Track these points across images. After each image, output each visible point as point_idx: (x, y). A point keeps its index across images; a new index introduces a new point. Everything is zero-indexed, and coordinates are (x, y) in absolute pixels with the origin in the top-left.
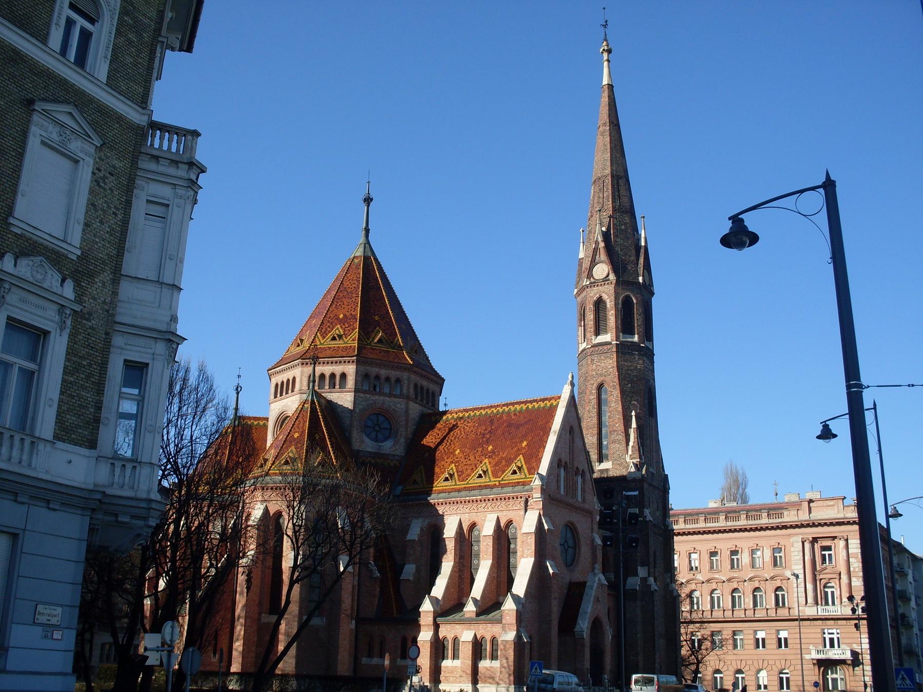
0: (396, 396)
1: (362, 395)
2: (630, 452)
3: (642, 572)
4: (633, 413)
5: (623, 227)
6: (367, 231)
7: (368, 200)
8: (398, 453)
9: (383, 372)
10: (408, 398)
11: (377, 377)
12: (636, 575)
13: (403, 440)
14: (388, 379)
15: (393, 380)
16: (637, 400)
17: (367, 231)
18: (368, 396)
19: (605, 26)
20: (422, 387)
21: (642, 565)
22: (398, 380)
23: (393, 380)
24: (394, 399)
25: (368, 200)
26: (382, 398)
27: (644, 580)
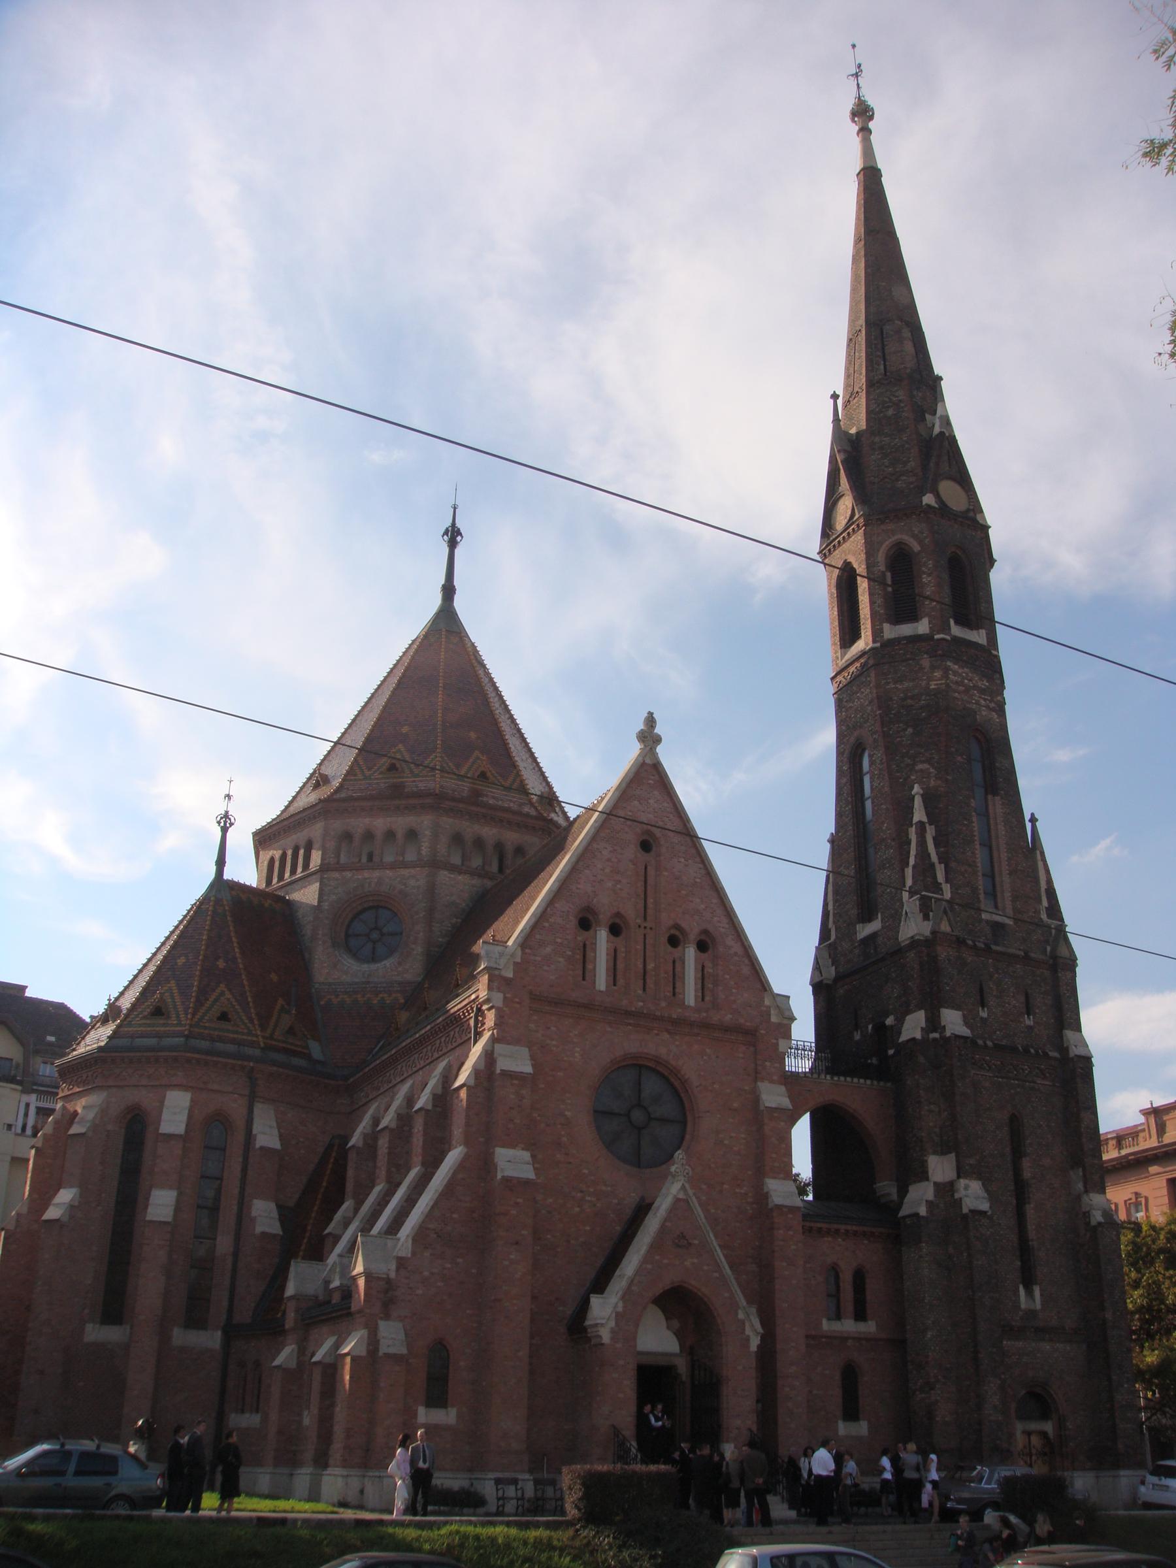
0: (405, 865)
1: (336, 875)
2: (909, 882)
3: (940, 1168)
4: (917, 789)
5: (890, 412)
6: (449, 590)
7: (453, 536)
8: (409, 977)
9: (380, 824)
10: (435, 864)
11: (369, 836)
12: (923, 1176)
13: (419, 949)
14: (390, 835)
15: (400, 835)
16: (929, 761)
17: (449, 590)
18: (348, 874)
19: (856, 75)
20: (479, 843)
21: (943, 1151)
22: (412, 835)
23: (400, 835)
24: (405, 872)
25: (453, 536)
26: (377, 874)
27: (946, 1190)
